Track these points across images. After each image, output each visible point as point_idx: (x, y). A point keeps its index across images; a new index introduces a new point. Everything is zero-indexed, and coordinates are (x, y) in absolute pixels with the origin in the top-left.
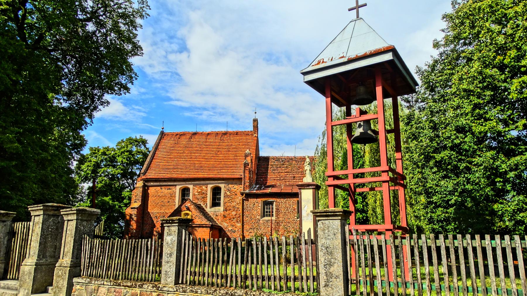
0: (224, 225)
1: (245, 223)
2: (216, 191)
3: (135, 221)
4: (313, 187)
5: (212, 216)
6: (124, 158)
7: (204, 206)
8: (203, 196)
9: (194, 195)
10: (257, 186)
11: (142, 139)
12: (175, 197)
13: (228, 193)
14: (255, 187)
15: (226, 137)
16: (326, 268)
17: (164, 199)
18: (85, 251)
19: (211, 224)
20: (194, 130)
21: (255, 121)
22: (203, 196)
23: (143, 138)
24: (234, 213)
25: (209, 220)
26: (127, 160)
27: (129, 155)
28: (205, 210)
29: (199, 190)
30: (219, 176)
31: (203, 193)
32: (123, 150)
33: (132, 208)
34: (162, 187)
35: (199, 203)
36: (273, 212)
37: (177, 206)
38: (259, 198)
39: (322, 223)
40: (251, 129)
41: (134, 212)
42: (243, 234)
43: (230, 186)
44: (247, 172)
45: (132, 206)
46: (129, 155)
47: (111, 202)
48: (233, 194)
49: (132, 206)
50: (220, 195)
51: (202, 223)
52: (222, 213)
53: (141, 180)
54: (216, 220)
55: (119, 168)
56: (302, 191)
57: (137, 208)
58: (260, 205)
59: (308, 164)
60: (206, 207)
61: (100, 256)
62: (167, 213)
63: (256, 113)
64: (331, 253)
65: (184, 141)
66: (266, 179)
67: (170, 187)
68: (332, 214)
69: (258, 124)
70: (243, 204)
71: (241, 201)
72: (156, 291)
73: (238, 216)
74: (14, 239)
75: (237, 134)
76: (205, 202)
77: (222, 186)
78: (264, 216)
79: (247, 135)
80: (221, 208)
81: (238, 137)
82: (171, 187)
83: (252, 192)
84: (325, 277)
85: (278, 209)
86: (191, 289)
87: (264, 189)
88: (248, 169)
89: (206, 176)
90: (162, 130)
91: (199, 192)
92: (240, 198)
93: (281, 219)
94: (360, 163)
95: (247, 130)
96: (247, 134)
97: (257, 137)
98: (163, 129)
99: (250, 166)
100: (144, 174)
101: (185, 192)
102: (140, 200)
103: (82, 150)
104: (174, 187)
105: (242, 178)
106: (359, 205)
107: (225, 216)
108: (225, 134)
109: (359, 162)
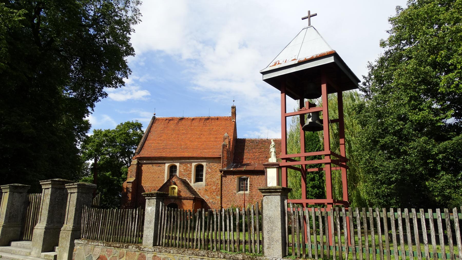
0: (206, 198)
1: (223, 197)
2: (199, 169)
3: (131, 193)
4: (277, 166)
5: (196, 190)
6: (122, 139)
7: (189, 182)
8: (188, 172)
9: (180, 172)
10: (235, 165)
11: (137, 123)
12: (164, 173)
13: (209, 170)
14: (232, 166)
15: (208, 121)
16: (269, 234)
17: (155, 175)
18: (84, 218)
19: (194, 197)
20: (181, 117)
21: (234, 108)
22: (188, 172)
23: (139, 122)
24: (214, 187)
25: (193, 194)
26: (125, 141)
27: (126, 136)
28: (189, 185)
29: (185, 168)
30: (202, 156)
31: (188, 170)
32: (121, 132)
33: (128, 182)
34: (153, 165)
35: (185, 179)
36: (247, 187)
37: (166, 181)
39: (267, 198)
40: (230, 115)
41: (130, 186)
42: (222, 205)
44: (225, 152)
45: (128, 181)
46: (126, 136)
47: (111, 177)
48: (214, 171)
49: (128, 181)
50: (203, 172)
51: (187, 196)
52: (204, 187)
53: (136, 159)
54: (199, 193)
56: (268, 169)
57: (132, 182)
58: (236, 181)
59: (273, 147)
60: (191, 182)
61: (96, 223)
62: (157, 187)
63: (234, 101)
64: (273, 222)
65: (172, 125)
66: (242, 159)
67: (160, 165)
68: (274, 190)
69: (235, 111)
70: (222, 180)
72: (139, 251)
73: (217, 190)
74: (28, 207)
75: (217, 120)
76: (190, 178)
77: (204, 164)
78: (239, 191)
79: (226, 120)
80: (203, 183)
81: (218, 122)
83: (230, 169)
84: (268, 241)
85: (252, 184)
86: (165, 249)
87: (240, 167)
88: (226, 149)
89: (190, 155)
91: (185, 169)
92: (219, 174)
94: (318, 146)
95: (226, 116)
96: (226, 119)
97: (235, 122)
99: (228, 147)
100: (139, 153)
101: (173, 169)
102: (135, 176)
103: (86, 132)
104: (163, 165)
105: (220, 158)
106: (317, 182)
107: (206, 190)
108: (208, 119)
109: (317, 145)
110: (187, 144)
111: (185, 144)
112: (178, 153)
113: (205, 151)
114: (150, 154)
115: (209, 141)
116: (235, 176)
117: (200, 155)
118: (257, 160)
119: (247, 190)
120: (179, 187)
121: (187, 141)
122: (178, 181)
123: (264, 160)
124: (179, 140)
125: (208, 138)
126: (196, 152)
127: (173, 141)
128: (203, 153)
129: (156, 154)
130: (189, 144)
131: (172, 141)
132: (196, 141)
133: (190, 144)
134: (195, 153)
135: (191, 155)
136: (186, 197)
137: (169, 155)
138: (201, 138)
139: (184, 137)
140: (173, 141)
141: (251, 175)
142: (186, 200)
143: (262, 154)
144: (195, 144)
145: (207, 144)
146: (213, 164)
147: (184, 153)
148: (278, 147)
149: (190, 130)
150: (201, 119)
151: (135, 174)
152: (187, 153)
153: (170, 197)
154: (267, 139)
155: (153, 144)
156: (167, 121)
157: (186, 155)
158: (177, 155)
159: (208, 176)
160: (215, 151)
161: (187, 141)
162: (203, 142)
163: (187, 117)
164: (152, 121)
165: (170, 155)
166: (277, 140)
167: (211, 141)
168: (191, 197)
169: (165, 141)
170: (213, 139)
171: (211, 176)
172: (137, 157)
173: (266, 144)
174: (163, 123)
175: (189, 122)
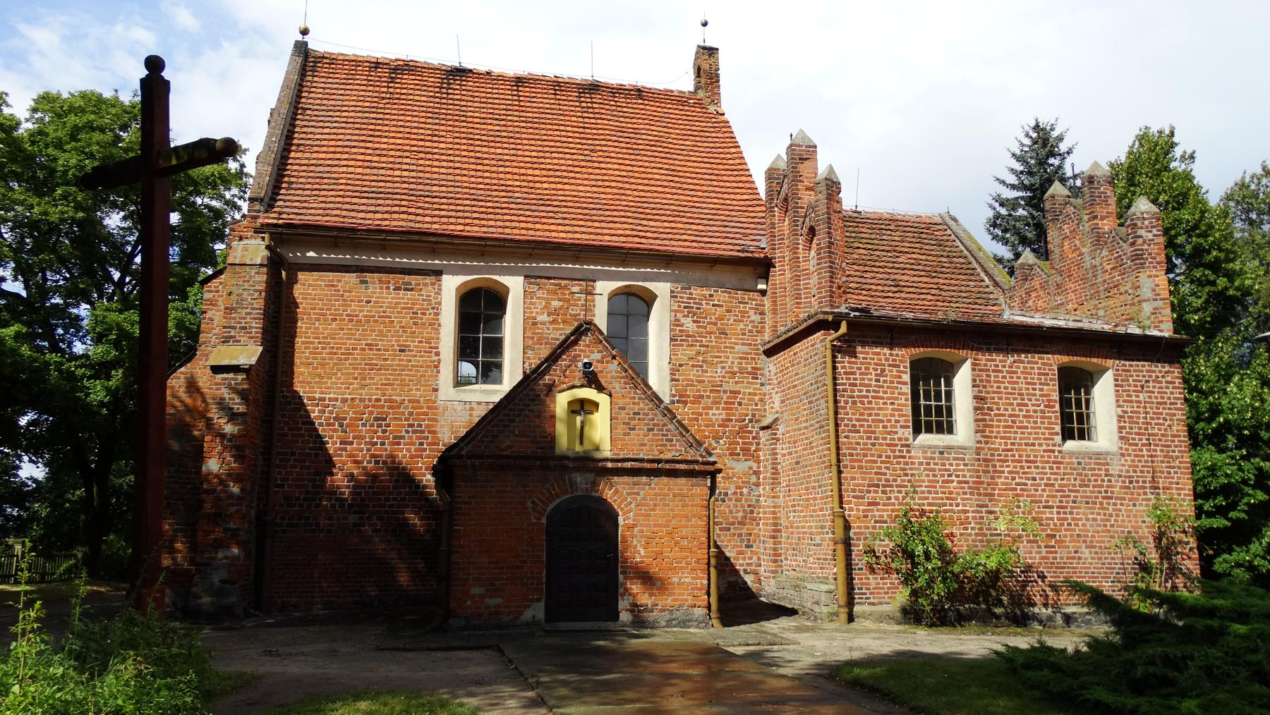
1: (846, 461)
12: (435, 325)
13: (688, 324)
15: (597, 98)
17: (381, 333)
20: (451, 61)
24: (717, 414)
29: (556, 304)
30: (647, 244)
38: (900, 346)
40: (684, 82)
43: (696, 292)
47: (25, 350)
50: (647, 335)
51: (668, 456)
55: (65, 197)
57: (247, 371)
63: (705, 24)
67: (407, 278)
71: (829, 360)
73: (734, 426)
75: (640, 97)
78: (917, 431)
81: (650, 108)
82: (413, 279)
89: (584, 238)
90: (300, 37)
91: (555, 312)
93: (998, 444)
98: (305, 32)
104: (428, 280)
108: (593, 88)
110: (538, 185)
111: (526, 184)
112: (508, 224)
113: (652, 223)
114: (344, 213)
115: (646, 182)
116: (904, 355)
117: (637, 240)
118: (864, 292)
119: (950, 430)
120: (621, 402)
121: (530, 172)
122: (614, 366)
123: (890, 294)
124: (486, 162)
125: (635, 169)
126: (603, 225)
127: (451, 164)
128: (649, 235)
129: (378, 216)
130: (545, 186)
131: (444, 164)
132: (578, 176)
133: (553, 186)
134: (605, 231)
135: (587, 237)
136: (668, 461)
137: (461, 228)
138: (596, 165)
139: (506, 151)
140: (451, 164)
141: (978, 349)
142: (665, 480)
143: (867, 268)
144: (581, 188)
145: (642, 194)
146: (706, 292)
147: (546, 227)
148: (917, 245)
149: (523, 124)
150: (557, 85)
151: (256, 326)
152: (561, 228)
153: (564, 457)
154: (855, 212)
155: (342, 169)
156: (384, 73)
157: (560, 234)
158: (507, 231)
159: (685, 353)
160: (701, 228)
161: (530, 172)
162: (620, 185)
163: (483, 68)
164: (300, 60)
165: (468, 228)
166: (899, 217)
167: (652, 182)
168: (696, 462)
169: (408, 160)
170: (664, 177)
171: (698, 353)
172: (268, 225)
173: (863, 230)
174: (361, 79)
175: (506, 91)
